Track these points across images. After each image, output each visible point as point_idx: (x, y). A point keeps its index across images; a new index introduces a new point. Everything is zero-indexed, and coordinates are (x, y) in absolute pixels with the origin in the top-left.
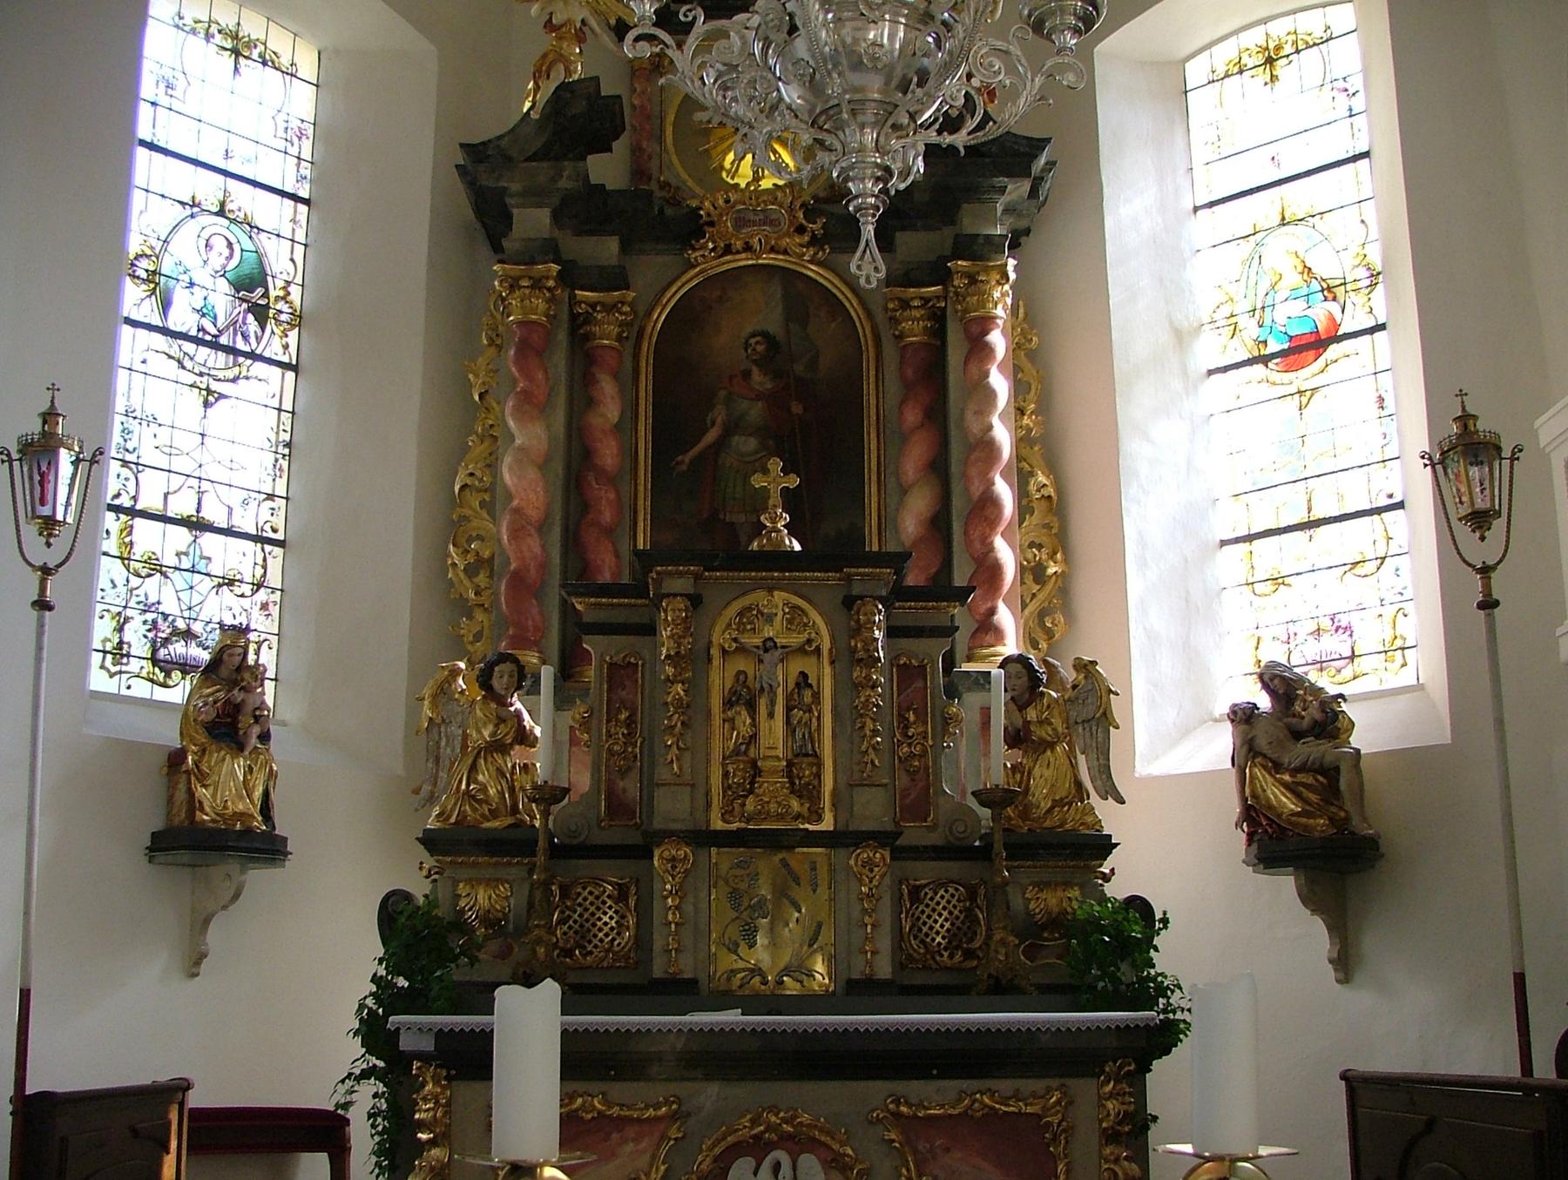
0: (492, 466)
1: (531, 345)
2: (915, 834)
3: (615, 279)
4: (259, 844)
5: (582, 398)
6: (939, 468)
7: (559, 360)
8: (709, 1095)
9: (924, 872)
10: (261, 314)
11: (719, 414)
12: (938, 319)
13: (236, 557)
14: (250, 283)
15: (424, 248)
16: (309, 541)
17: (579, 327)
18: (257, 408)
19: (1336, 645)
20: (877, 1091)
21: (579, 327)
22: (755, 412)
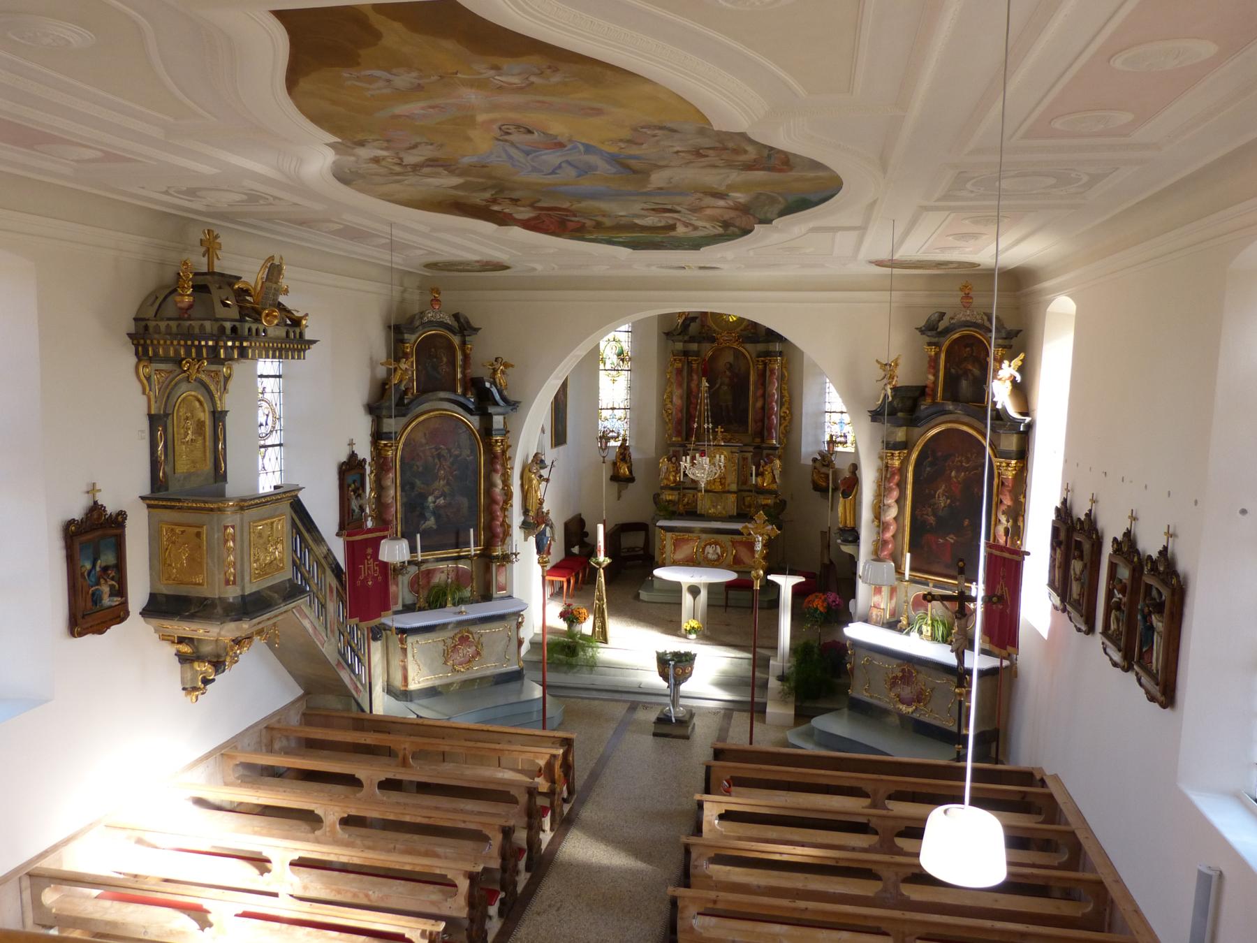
0: (671, 393)
1: (679, 372)
2: (745, 487)
3: (697, 354)
4: (631, 479)
5: (690, 381)
6: (763, 395)
7: (685, 373)
8: (704, 536)
9: (745, 494)
10: (623, 360)
11: (719, 381)
12: (765, 364)
13: (620, 413)
14: (620, 354)
15: (655, 355)
16: (635, 408)
17: (689, 363)
18: (623, 379)
19: (842, 439)
20: (729, 537)
21: (689, 363)
22: (727, 380)
